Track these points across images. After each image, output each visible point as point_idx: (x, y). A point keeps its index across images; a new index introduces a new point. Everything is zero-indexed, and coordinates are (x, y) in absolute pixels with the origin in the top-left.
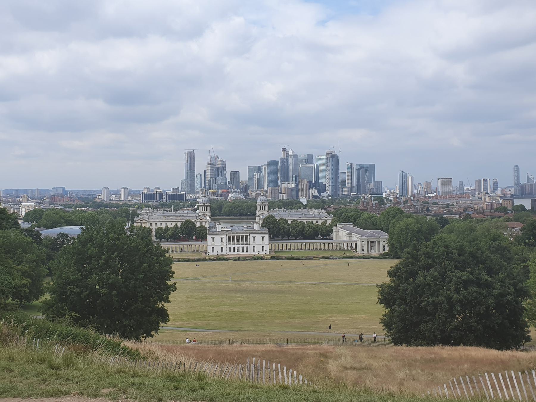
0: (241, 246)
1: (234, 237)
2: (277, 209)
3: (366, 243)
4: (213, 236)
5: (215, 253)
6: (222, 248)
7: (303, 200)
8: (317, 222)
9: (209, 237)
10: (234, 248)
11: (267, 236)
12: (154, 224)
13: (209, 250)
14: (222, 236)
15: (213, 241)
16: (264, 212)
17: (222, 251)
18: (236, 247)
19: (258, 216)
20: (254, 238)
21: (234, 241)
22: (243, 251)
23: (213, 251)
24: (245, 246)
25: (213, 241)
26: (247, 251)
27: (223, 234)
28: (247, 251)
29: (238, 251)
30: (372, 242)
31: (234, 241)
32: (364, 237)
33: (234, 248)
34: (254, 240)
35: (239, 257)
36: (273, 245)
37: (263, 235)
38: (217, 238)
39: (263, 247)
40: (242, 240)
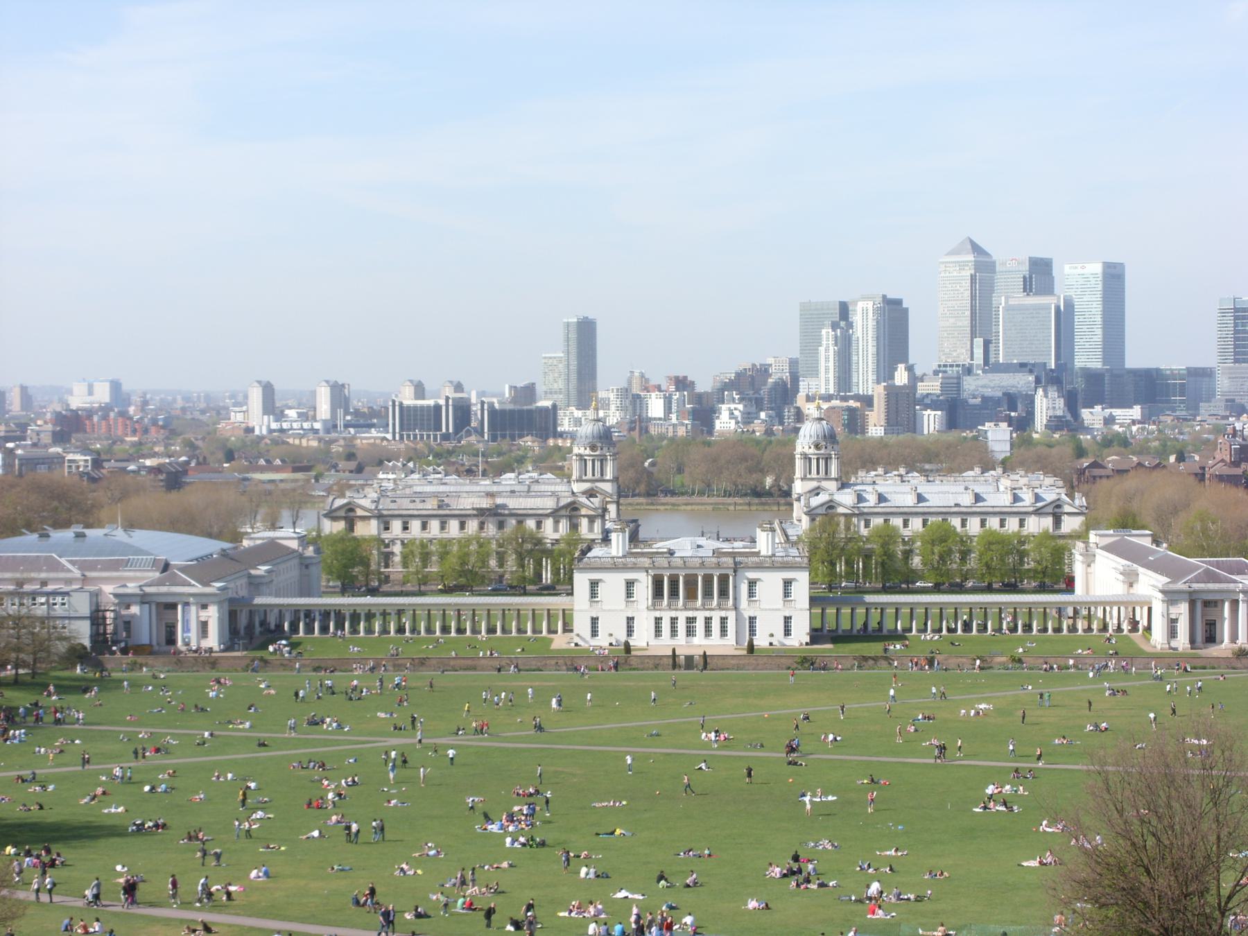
0: (700, 616)
2: (880, 471)
3: (1182, 610)
4: (595, 576)
5: (602, 641)
6: (630, 620)
7: (998, 436)
8: (1022, 524)
9: (581, 581)
10: (674, 621)
11: (802, 581)
12: (396, 525)
13: (581, 625)
14: (631, 576)
15: (593, 594)
16: (824, 484)
17: (630, 631)
18: (682, 617)
20: (752, 584)
21: (674, 593)
23: (594, 633)
24: (716, 616)
25: (593, 594)
26: (724, 631)
27: (634, 568)
28: (724, 631)
29: (690, 632)
30: (1207, 604)
31: (674, 593)
32: (1180, 586)
33: (674, 621)
34: (751, 594)
35: (689, 659)
36: (831, 611)
38: (613, 584)
39: (787, 620)
40: (708, 594)
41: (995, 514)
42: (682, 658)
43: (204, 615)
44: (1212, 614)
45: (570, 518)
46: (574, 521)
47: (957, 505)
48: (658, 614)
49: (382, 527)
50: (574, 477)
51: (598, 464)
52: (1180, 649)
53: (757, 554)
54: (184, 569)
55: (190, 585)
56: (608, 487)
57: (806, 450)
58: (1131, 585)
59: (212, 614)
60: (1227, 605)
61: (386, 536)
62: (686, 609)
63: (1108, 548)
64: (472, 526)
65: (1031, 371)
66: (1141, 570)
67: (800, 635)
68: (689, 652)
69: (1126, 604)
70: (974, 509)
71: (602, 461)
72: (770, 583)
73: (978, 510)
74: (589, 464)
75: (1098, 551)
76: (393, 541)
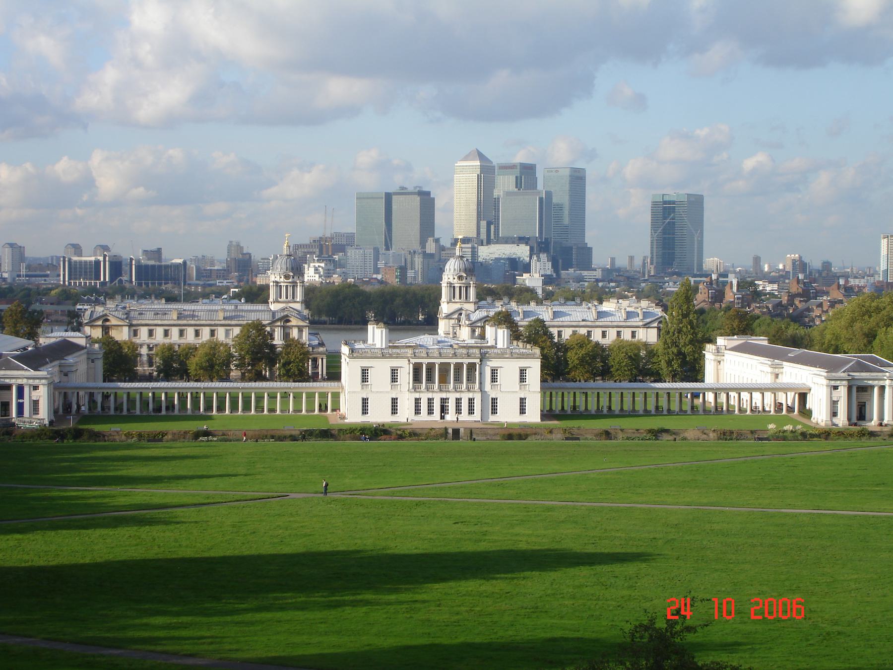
0: (452, 398)
1: (430, 368)
3: (842, 392)
4: (365, 363)
6: (394, 401)
8: (633, 334)
10: (430, 401)
11: (534, 368)
12: (144, 332)
14: (395, 363)
15: (364, 379)
17: (394, 411)
18: (437, 398)
19: (448, 317)
20: (494, 372)
21: (430, 379)
22: (458, 410)
23: (365, 411)
25: (364, 379)
26: (471, 411)
28: (471, 411)
29: (444, 410)
31: (430, 379)
33: (430, 401)
34: (494, 379)
37: (523, 363)
38: (380, 370)
39: (522, 401)
40: (458, 379)
41: (613, 327)
42: (450, 431)
43: (35, 395)
44: (864, 396)
45: (284, 327)
46: (287, 330)
47: (583, 320)
48: (417, 395)
49: (132, 334)
50: (271, 300)
51: (290, 290)
52: (840, 425)
53: (494, 347)
54: (16, 358)
55: (23, 369)
56: (298, 306)
57: (451, 280)
58: (777, 376)
59: (42, 395)
60: (876, 390)
61: (137, 340)
62: (441, 391)
63: (736, 349)
64: (205, 333)
65: (527, 244)
66: (784, 363)
67: (533, 416)
68: (456, 426)
69: (774, 390)
70: (597, 324)
71: (293, 287)
72: (509, 369)
73: (601, 324)
74: (284, 289)
75: (726, 352)
76: (141, 345)
